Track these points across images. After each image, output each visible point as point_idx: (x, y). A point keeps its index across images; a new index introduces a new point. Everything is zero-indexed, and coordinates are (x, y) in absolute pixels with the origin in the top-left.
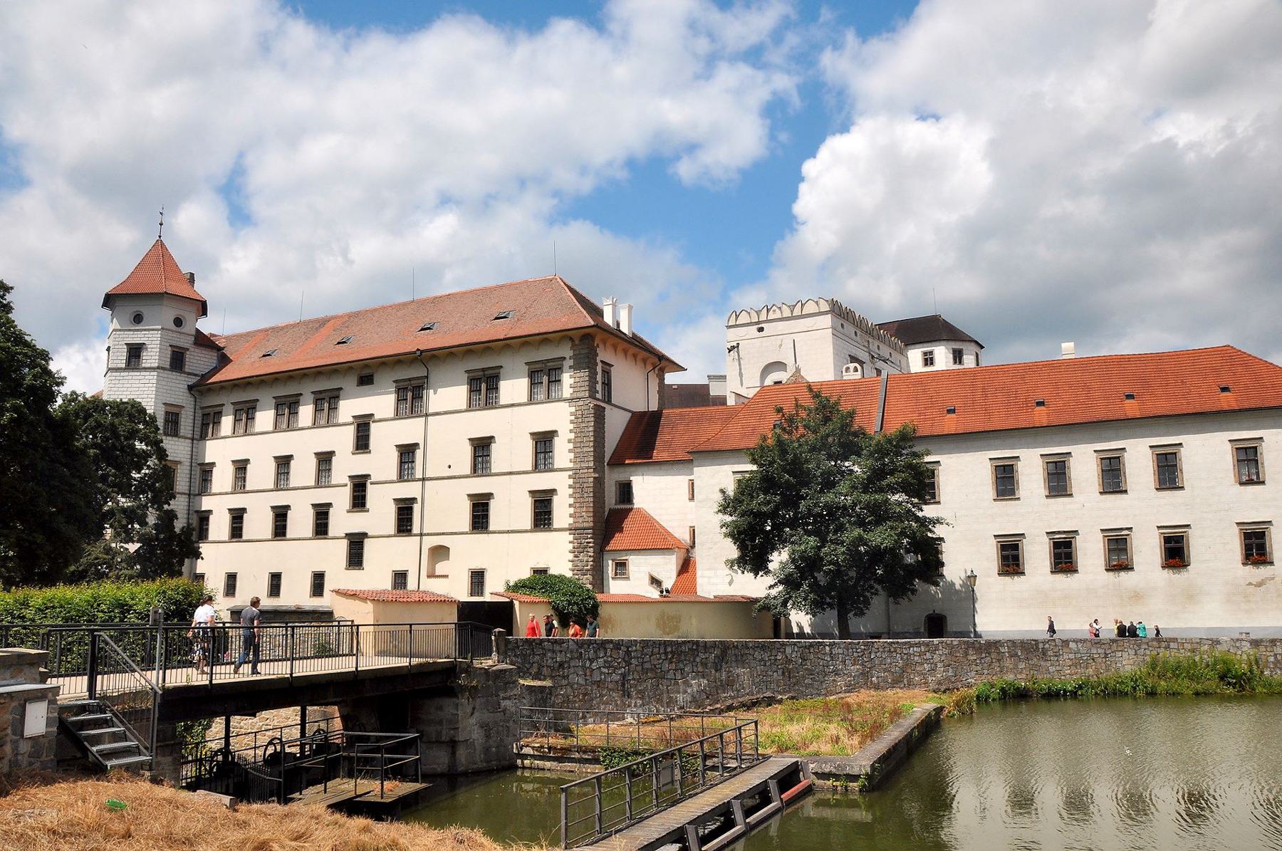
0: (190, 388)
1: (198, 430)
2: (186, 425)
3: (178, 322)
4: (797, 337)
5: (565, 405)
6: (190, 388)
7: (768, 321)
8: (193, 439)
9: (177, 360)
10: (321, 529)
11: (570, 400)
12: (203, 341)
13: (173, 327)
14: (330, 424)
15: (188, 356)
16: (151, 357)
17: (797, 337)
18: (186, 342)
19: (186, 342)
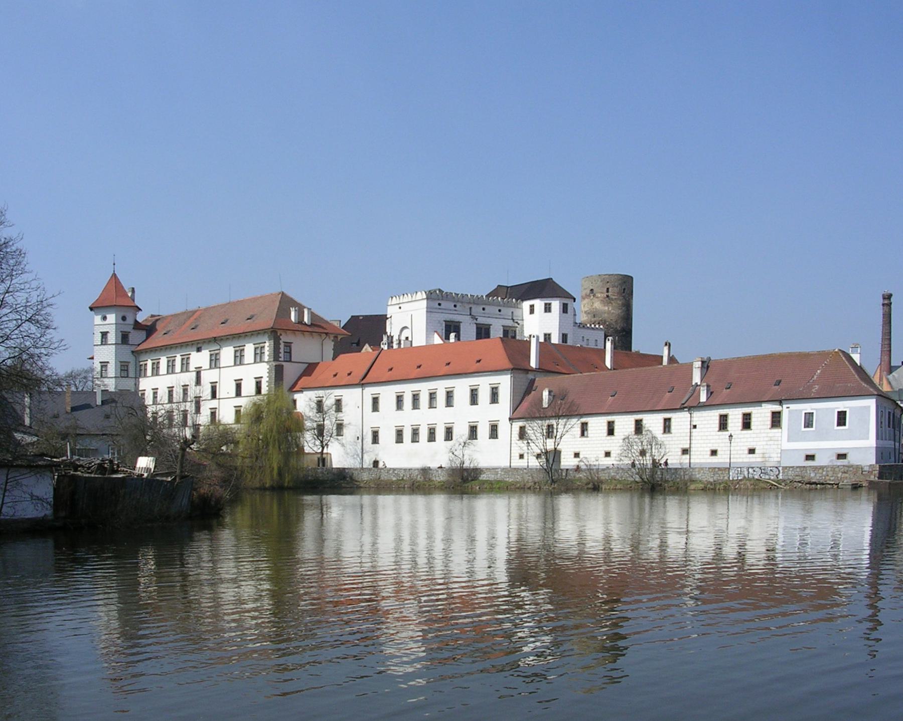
2: (132, 373)
3: (124, 318)
5: (265, 364)
6: (133, 352)
9: (124, 338)
12: (137, 326)
13: (122, 322)
14: (187, 371)
15: (130, 335)
16: (112, 338)
18: (129, 329)
19: (129, 329)
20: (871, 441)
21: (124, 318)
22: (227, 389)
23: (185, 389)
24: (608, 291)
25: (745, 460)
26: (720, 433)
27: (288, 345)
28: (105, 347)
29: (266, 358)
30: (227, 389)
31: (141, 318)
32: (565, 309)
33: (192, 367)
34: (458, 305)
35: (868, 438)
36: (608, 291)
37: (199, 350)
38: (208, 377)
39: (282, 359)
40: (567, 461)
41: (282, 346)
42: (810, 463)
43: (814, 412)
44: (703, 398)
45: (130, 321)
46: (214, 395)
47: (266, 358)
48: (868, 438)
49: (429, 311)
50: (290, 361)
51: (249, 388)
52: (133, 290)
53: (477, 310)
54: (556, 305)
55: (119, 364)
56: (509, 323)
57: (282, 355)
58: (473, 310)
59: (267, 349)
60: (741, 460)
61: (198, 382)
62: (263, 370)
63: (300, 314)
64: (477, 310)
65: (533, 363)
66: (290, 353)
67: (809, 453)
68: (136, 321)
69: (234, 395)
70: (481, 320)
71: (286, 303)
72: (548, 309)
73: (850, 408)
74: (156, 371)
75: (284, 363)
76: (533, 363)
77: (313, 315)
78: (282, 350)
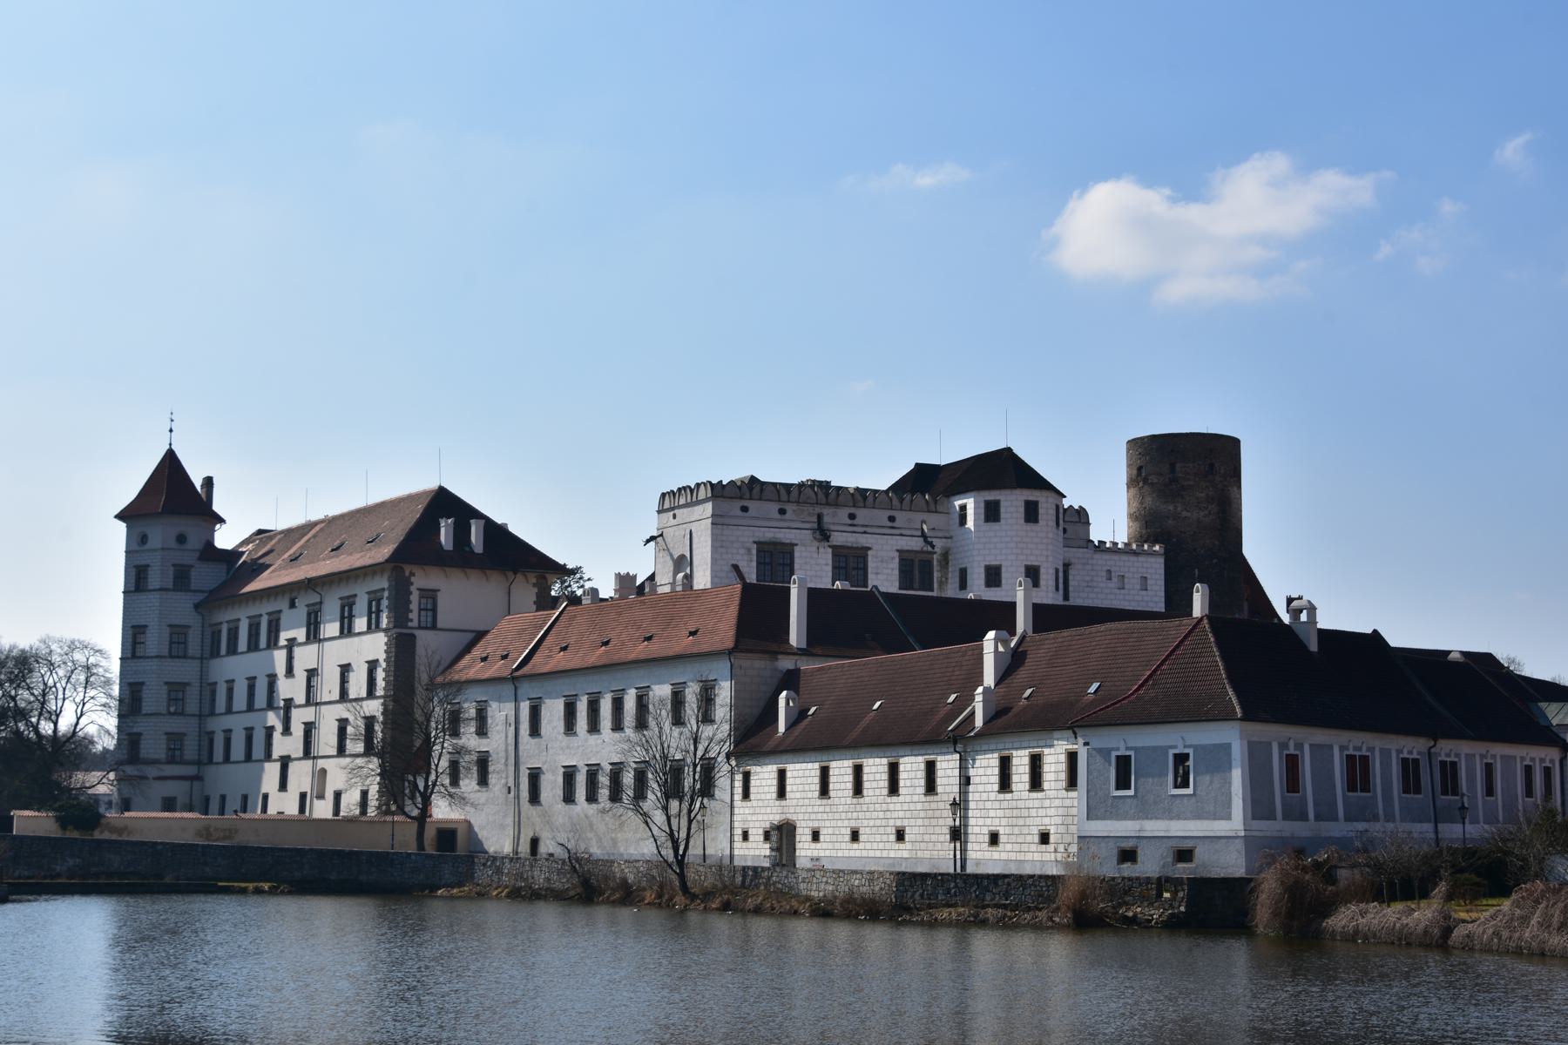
0: (197, 606)
1: (207, 649)
2: (194, 647)
3: (181, 539)
4: (694, 527)
5: (382, 635)
6: (197, 606)
7: (680, 507)
8: (202, 658)
9: (181, 578)
10: (268, 756)
11: (385, 631)
13: (173, 544)
15: (193, 573)
16: (154, 580)
17: (694, 527)
18: (188, 558)
20: (1235, 823)
21: (181, 539)
22: (329, 687)
23: (272, 679)
24: (1173, 466)
25: (1037, 857)
26: (1001, 796)
27: (430, 595)
28: (142, 596)
29: (384, 622)
30: (329, 687)
31: (225, 539)
32: (1031, 513)
33: (282, 642)
34: (790, 508)
35: (1228, 817)
36: (1173, 466)
37: (292, 605)
38: (306, 657)
39: (415, 624)
40: (805, 850)
41: (415, 598)
42: (1128, 870)
43: (1190, 751)
44: (979, 722)
45: (195, 542)
46: (309, 702)
47: (384, 622)
48: (1228, 817)
49: (718, 521)
50: (434, 627)
51: (358, 686)
52: (209, 482)
53: (835, 517)
54: (1012, 502)
55: (167, 631)
56: (916, 544)
57: (414, 615)
58: (826, 519)
59: (385, 603)
60: (1029, 857)
61: (290, 672)
62: (375, 646)
63: (461, 533)
64: (835, 517)
65: (795, 637)
66: (434, 610)
67: (1128, 845)
68: (210, 544)
69: (336, 695)
70: (838, 538)
71: (443, 503)
72: (991, 513)
73: (1196, 748)
74: (233, 650)
75: (419, 634)
76: (795, 637)
77: (497, 534)
78: (414, 606)
